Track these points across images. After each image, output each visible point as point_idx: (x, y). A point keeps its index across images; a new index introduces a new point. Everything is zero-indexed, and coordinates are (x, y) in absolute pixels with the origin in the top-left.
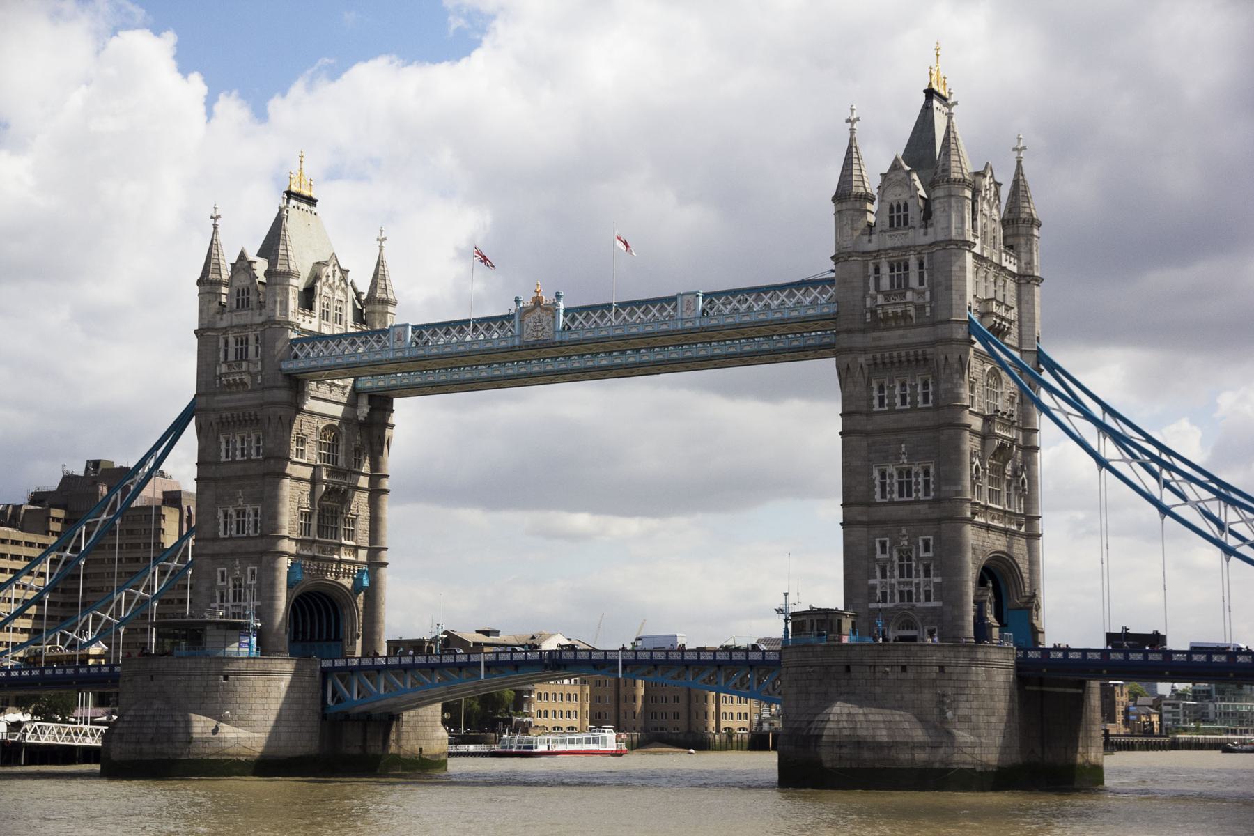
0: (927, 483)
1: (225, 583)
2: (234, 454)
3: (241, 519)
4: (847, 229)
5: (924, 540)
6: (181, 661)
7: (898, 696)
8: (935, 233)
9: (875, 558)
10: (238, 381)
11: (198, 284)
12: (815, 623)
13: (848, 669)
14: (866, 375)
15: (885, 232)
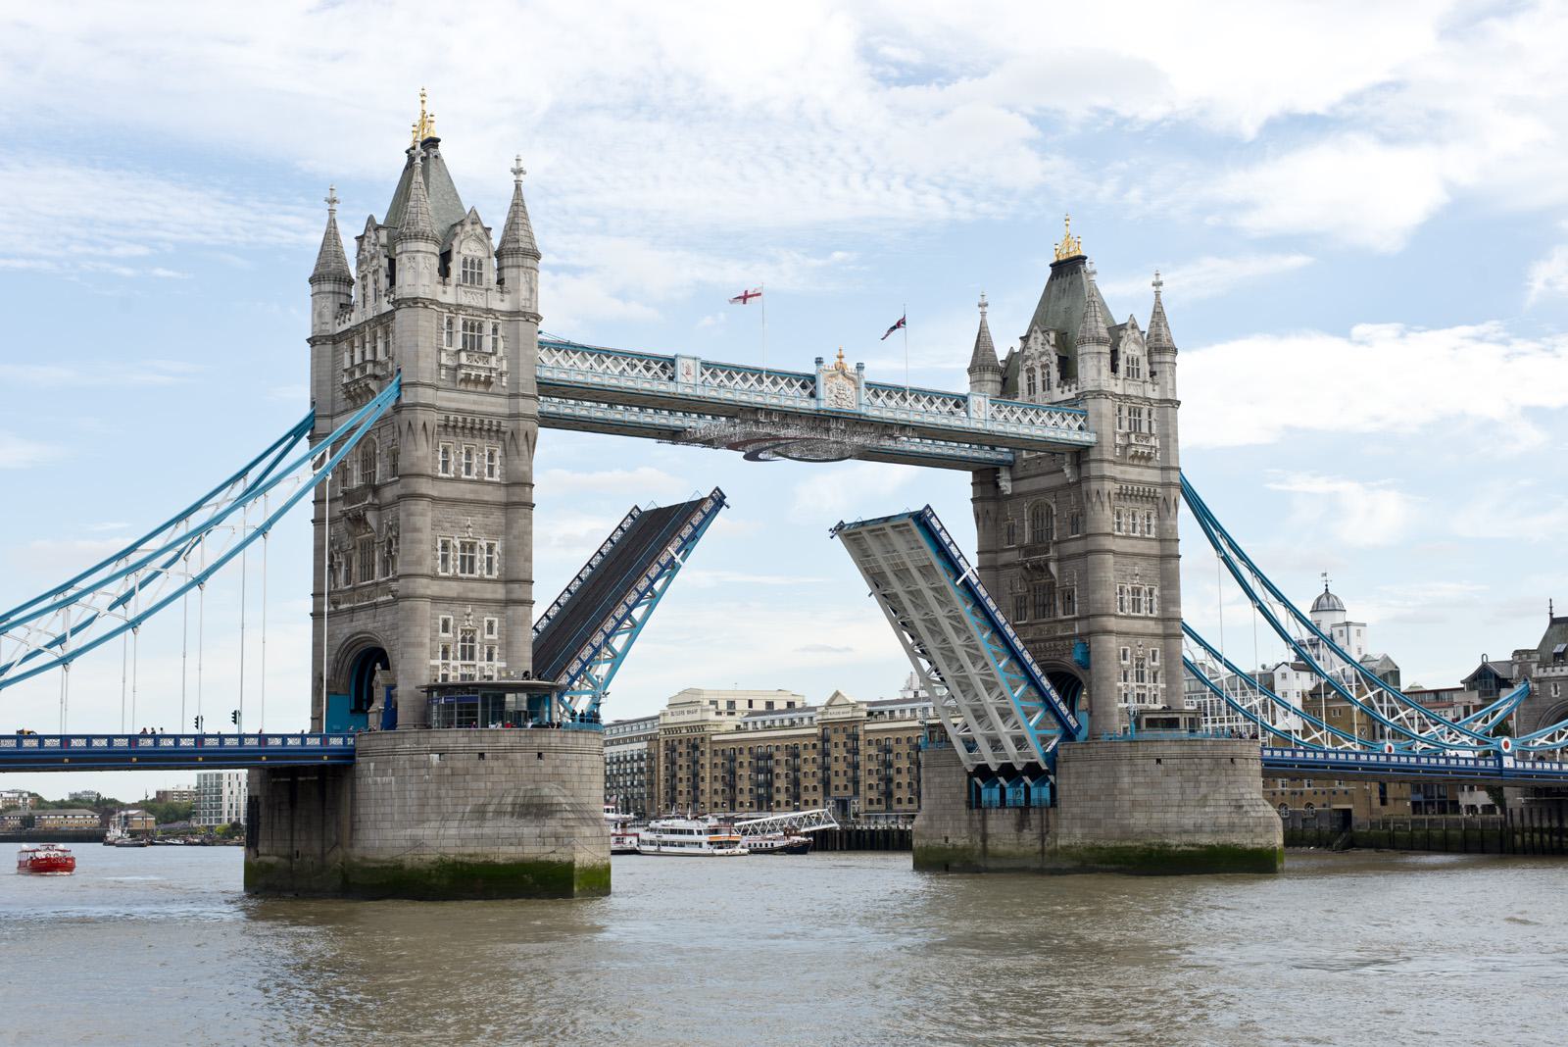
0: (1151, 601)
1: (450, 635)
3: (468, 554)
6: (575, 735)
8: (1163, 390)
13: (1232, 759)
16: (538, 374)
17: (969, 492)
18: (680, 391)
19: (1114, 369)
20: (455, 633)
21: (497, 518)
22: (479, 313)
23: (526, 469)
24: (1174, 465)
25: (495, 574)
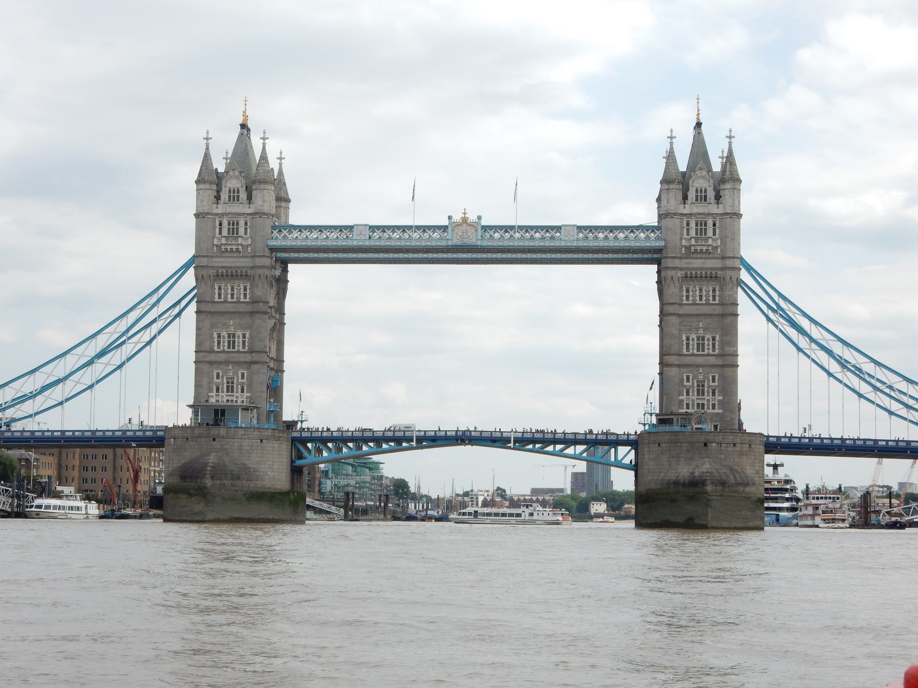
0: (714, 345)
1: (220, 380)
2: (226, 297)
3: (231, 339)
4: (673, 202)
5: (712, 376)
6: (236, 429)
7: (732, 460)
8: (725, 208)
9: (683, 385)
10: (234, 250)
11: (197, 182)
12: (680, 419)
13: (705, 445)
14: (680, 283)
15: (694, 203)
16: (269, 243)
17: (655, 278)
18: (355, 243)
19: (685, 198)
20: (223, 380)
21: (247, 320)
22: (235, 216)
23: (260, 294)
24: (728, 256)
25: (247, 348)
